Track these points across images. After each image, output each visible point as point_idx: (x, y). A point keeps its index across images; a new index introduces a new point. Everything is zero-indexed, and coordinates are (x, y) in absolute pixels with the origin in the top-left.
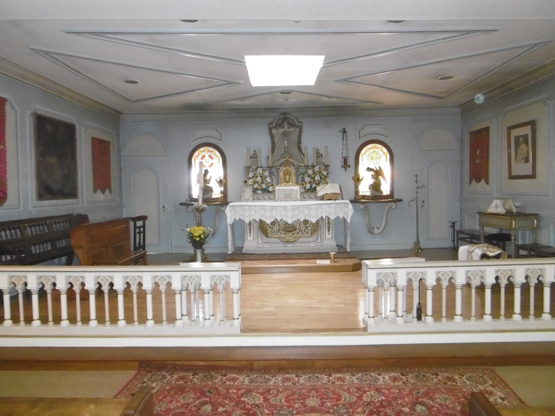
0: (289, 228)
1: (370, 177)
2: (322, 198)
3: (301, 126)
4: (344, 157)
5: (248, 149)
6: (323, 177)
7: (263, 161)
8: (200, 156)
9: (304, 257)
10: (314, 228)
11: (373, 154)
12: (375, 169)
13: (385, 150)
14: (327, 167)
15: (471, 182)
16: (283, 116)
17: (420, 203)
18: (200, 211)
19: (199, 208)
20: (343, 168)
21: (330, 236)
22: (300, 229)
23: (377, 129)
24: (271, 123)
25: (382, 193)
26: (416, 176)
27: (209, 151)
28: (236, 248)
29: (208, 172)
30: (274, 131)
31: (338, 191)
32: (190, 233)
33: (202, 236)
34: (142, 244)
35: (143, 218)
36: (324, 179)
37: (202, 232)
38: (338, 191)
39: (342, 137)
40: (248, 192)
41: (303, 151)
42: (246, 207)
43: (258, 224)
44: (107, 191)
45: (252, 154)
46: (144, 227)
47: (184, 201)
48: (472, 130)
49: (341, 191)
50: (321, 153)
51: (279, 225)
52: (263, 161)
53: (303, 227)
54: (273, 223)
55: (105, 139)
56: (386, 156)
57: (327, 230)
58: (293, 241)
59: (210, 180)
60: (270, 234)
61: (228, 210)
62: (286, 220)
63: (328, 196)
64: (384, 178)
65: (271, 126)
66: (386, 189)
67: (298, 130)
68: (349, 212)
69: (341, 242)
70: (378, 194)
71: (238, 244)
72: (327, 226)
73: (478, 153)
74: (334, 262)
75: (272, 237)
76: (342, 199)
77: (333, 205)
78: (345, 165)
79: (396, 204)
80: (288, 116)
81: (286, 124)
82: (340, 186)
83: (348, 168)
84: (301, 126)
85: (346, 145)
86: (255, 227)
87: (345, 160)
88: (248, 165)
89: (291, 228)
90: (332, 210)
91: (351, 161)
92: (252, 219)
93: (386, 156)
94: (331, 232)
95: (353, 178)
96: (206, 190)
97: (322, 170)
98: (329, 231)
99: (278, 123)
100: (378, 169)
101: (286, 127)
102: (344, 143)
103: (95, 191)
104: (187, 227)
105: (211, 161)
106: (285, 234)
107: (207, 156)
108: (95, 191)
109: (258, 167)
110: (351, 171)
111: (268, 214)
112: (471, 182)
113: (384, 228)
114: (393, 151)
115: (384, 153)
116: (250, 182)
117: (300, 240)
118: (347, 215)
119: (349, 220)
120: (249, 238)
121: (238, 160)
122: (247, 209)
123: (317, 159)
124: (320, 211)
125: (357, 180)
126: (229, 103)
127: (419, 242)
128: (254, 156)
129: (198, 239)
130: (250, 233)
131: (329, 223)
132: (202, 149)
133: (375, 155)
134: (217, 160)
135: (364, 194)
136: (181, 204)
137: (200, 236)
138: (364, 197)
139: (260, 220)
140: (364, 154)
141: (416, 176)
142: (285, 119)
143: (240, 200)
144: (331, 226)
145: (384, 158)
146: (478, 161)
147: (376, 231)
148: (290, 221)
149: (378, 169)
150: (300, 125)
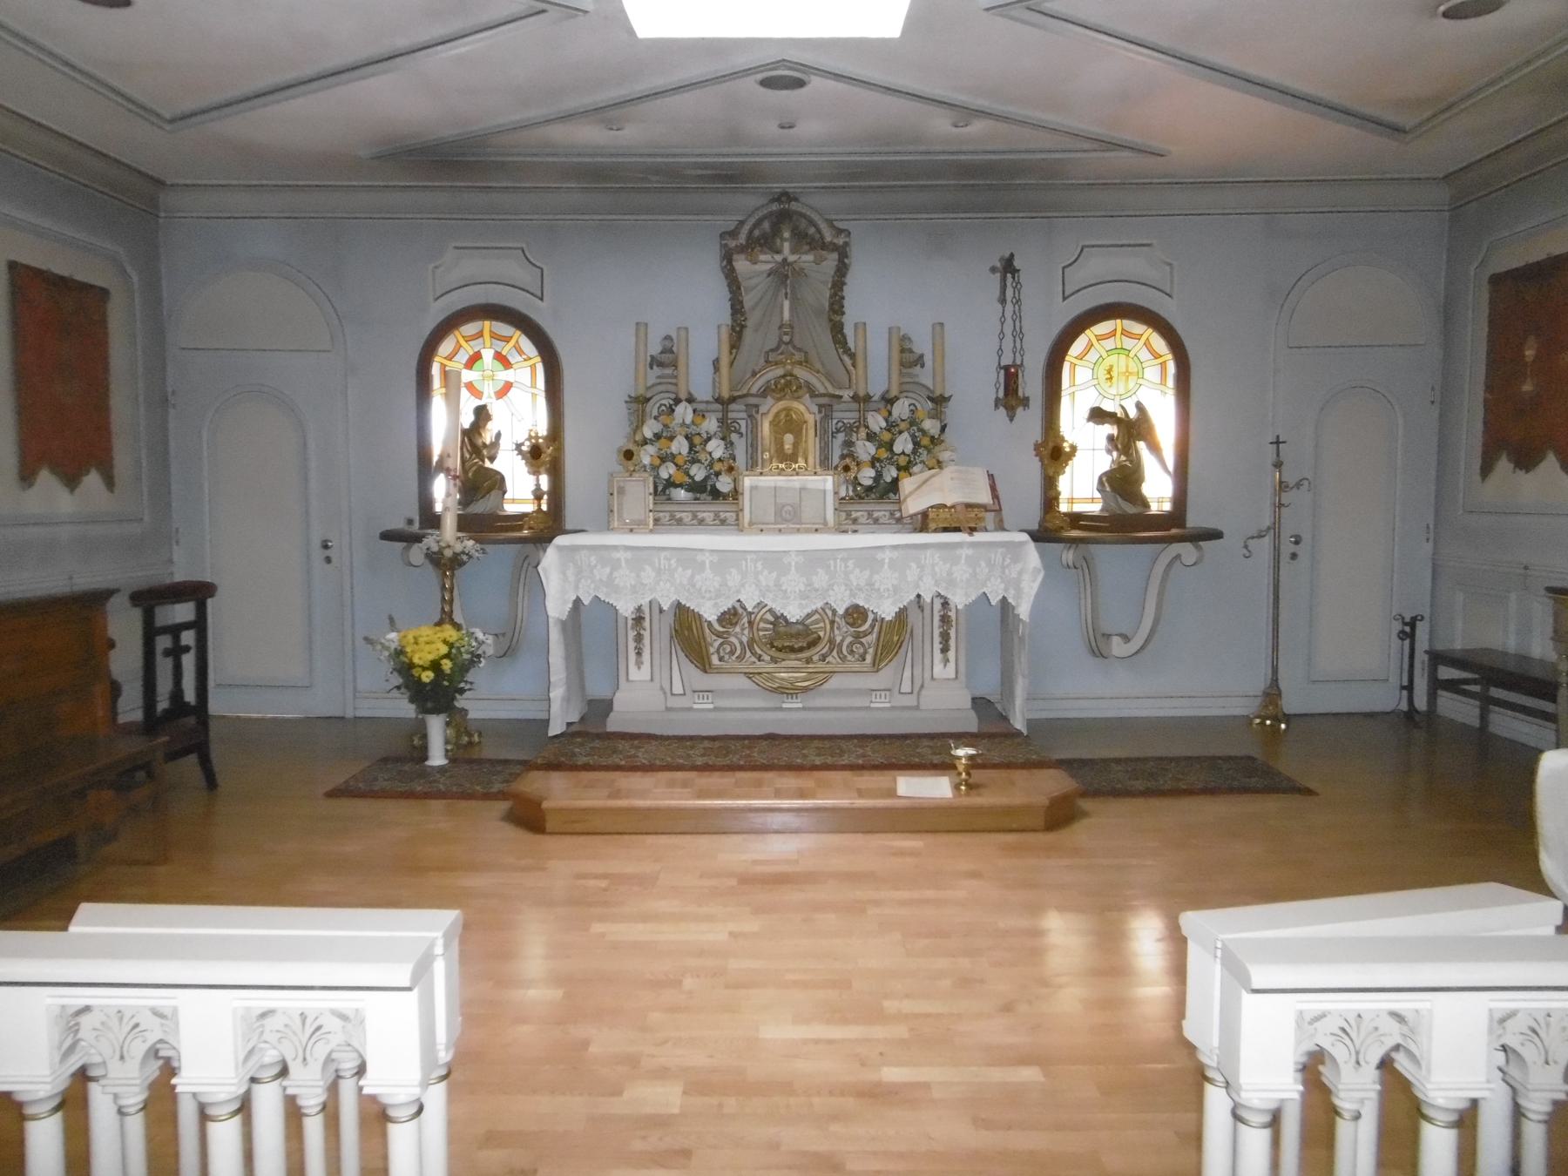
0: (791, 639)
1: (1103, 443)
2: (923, 522)
3: (846, 244)
4: (1006, 368)
5: (641, 328)
6: (926, 441)
7: (700, 380)
8: (463, 357)
9: (845, 761)
10: (890, 640)
11: (1113, 359)
12: (1120, 414)
13: (1159, 344)
14: (940, 401)
15: (1486, 469)
16: (775, 207)
17: (1283, 545)
18: (446, 564)
19: (440, 552)
20: (1002, 410)
21: (950, 671)
22: (831, 641)
23: (1133, 264)
24: (733, 234)
25: (1146, 505)
26: (1277, 443)
27: (495, 336)
28: (591, 702)
29: (488, 418)
30: (741, 264)
31: (984, 497)
32: (400, 652)
33: (447, 665)
34: (190, 696)
35: (199, 593)
36: (928, 450)
37: (444, 650)
38: (984, 497)
39: (997, 293)
40: (639, 492)
41: (851, 344)
42: (621, 555)
43: (669, 619)
44: (92, 480)
45: (655, 348)
46: (199, 624)
47: (398, 524)
48: (1502, 269)
49: (995, 496)
50: (918, 350)
51: (750, 622)
52: (700, 380)
53: (843, 634)
54: (730, 617)
55: (79, 277)
56: (1163, 365)
57: (937, 647)
58: (806, 690)
59: (495, 444)
60: (715, 660)
61: (550, 560)
62: (779, 609)
63: (944, 514)
64: (1155, 448)
65: (732, 244)
66: (1158, 490)
67: (832, 260)
68: (1026, 577)
69: (989, 686)
70: (1130, 509)
71: (597, 690)
72: (937, 632)
73: (1529, 353)
74: (970, 786)
75: (719, 671)
76: (1001, 527)
77: (965, 552)
78: (1010, 397)
79: (1199, 548)
80: (794, 206)
81: (786, 235)
82: (991, 477)
83: (1020, 410)
84: (846, 244)
85: (1017, 316)
86: (659, 631)
87: (1011, 378)
88: (641, 391)
89: (797, 635)
90: (961, 572)
91: (1032, 385)
92: (645, 602)
93: (1163, 365)
94: (951, 654)
95: (1037, 447)
96: (479, 482)
97: (920, 414)
98: (945, 650)
99: (757, 233)
100: (1133, 413)
101: (786, 245)
102: (1009, 314)
103: (27, 476)
104: (392, 624)
105: (504, 375)
106: (774, 660)
107: (488, 355)
108: (27, 476)
109: (677, 401)
110: (1030, 420)
111: (708, 579)
112: (1486, 469)
113: (1147, 641)
114: (1187, 344)
115: (1156, 356)
116: (647, 456)
117: (835, 682)
118: (1019, 590)
119: (1024, 610)
120: (635, 674)
121: (606, 373)
122: (627, 562)
123: (901, 374)
124: (912, 573)
125: (1055, 455)
126: (558, 133)
127: (1280, 694)
128: (667, 359)
129: (427, 677)
130: (639, 654)
131: (945, 619)
132: (470, 328)
133: (1117, 362)
134: (527, 374)
135: (1078, 508)
136: (388, 536)
137: (435, 666)
138: (1076, 519)
139: (680, 609)
140: (1081, 357)
141: (1277, 443)
142: (783, 217)
143: (608, 528)
144: (952, 632)
145: (1152, 373)
146: (1527, 387)
147: (1118, 647)
148: (794, 613)
149: (1133, 413)
150: (840, 241)
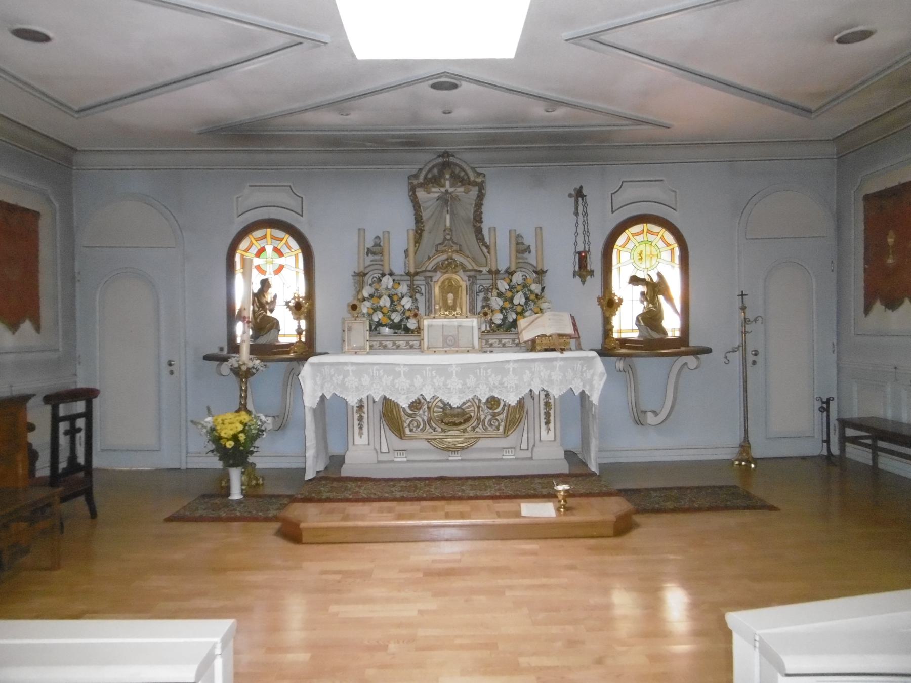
0: (454, 418)
1: (638, 296)
2: (532, 346)
3: (483, 182)
4: (580, 253)
5: (361, 231)
6: (532, 297)
7: (397, 262)
8: (254, 250)
9: (488, 493)
10: (514, 417)
11: (642, 247)
13: (669, 238)
14: (540, 273)
15: (867, 310)
16: (440, 160)
17: (748, 357)
18: (243, 375)
19: (239, 367)
21: (551, 436)
22: (478, 419)
23: (655, 191)
24: (416, 176)
25: (665, 333)
27: (274, 238)
28: (332, 458)
29: (269, 286)
30: (421, 194)
31: (569, 330)
32: (213, 429)
33: (242, 437)
34: (81, 460)
35: (89, 395)
36: (534, 301)
37: (240, 427)
38: (569, 330)
40: (360, 330)
41: (487, 240)
42: (349, 368)
43: (379, 407)
45: (370, 244)
46: (88, 415)
47: (214, 350)
49: (576, 329)
50: (527, 243)
51: (429, 408)
52: (397, 262)
53: (486, 414)
54: (416, 405)
56: (672, 250)
57: (543, 421)
58: (463, 448)
59: (273, 302)
60: (407, 431)
61: (306, 371)
62: (446, 400)
63: (545, 341)
64: (669, 299)
65: (415, 182)
66: (672, 324)
67: (474, 192)
68: (596, 378)
69: (574, 444)
70: (656, 336)
71: (335, 450)
72: (542, 411)
74: (567, 509)
75: (411, 438)
76: (579, 348)
77: (558, 364)
78: (583, 269)
79: (698, 359)
80: (452, 159)
81: (448, 176)
82: (573, 318)
84: (483, 182)
85: (586, 223)
86: (373, 415)
88: (362, 269)
89: (457, 415)
90: (556, 376)
91: (595, 262)
92: (364, 396)
93: (672, 250)
94: (552, 426)
95: (599, 299)
96: (264, 325)
97: (529, 281)
98: (547, 423)
99: (430, 176)
100: (655, 279)
101: (448, 183)
104: (209, 412)
105: (279, 261)
106: (443, 431)
107: (269, 249)
109: (383, 275)
110: (595, 283)
111: (403, 382)
112: (867, 310)
113: (668, 416)
115: (668, 245)
116: (365, 308)
117: (481, 443)
119: (595, 398)
120: (358, 440)
121: (340, 260)
122: (354, 373)
123: (517, 257)
124: (527, 377)
125: (610, 304)
126: (312, 118)
128: (377, 250)
129: (230, 444)
130: (361, 428)
131: (547, 404)
132: (258, 233)
134: (293, 260)
135: (624, 336)
136: (207, 358)
137: (235, 438)
138: (623, 342)
139: (386, 401)
140: (623, 246)
141: (742, 295)
142: (446, 165)
143: (341, 351)
144: (552, 412)
145: (666, 255)
146: (890, 261)
147: (650, 419)
148: (455, 401)
150: (479, 180)
